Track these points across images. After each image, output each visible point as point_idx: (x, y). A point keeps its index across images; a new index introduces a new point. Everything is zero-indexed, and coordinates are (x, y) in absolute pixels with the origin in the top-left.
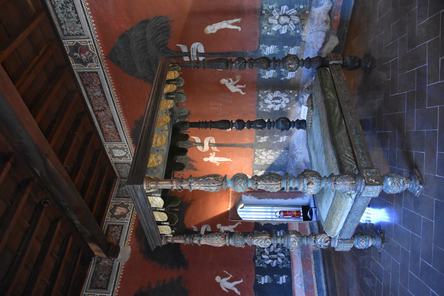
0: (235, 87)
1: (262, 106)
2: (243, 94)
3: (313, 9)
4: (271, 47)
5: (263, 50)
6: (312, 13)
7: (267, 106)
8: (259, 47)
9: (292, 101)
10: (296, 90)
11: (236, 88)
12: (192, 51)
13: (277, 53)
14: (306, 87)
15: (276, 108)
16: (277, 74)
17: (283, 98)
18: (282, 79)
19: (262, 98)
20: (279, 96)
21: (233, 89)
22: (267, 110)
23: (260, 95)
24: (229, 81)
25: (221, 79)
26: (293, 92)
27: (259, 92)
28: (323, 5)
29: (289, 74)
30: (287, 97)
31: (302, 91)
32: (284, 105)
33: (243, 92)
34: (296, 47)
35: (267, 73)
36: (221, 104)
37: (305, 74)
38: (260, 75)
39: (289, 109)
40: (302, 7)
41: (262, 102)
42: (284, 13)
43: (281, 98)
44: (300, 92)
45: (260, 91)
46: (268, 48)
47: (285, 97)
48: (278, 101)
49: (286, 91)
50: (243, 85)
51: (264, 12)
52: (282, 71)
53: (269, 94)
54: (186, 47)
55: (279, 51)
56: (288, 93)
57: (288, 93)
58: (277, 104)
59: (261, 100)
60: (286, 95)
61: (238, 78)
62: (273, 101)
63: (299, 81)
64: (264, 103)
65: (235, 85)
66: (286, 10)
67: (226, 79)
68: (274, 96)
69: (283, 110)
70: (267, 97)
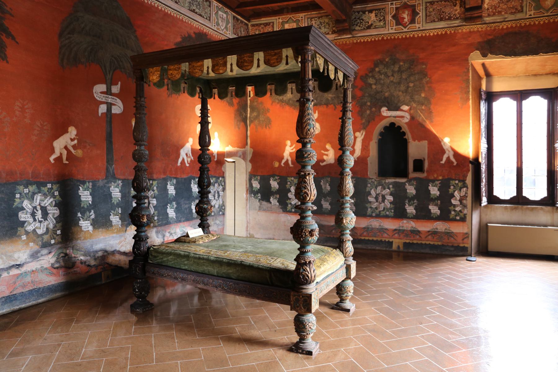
0: (63, 147)
1: (26, 191)
2: (52, 159)
3: (155, 230)
4: (119, 194)
5: (116, 184)
6: (152, 230)
7: (28, 199)
8: (119, 179)
9: (40, 239)
10: (62, 238)
11: (60, 149)
12: (113, 99)
13: (113, 202)
14: (68, 251)
15: (23, 216)
16: (86, 206)
17: (46, 223)
18: (79, 215)
19: (45, 189)
20: (50, 215)
21: (59, 145)
22: (17, 201)
23: (49, 186)
24: (72, 140)
25: (76, 128)
26: (58, 235)
27: (55, 184)
28: (158, 237)
29: (86, 222)
30: (47, 229)
31: (60, 248)
32: (30, 228)
33: (55, 159)
34: (120, 223)
35: (87, 193)
36: (28, 121)
37: (88, 244)
38: (84, 183)
39: (24, 237)
40: (156, 218)
41: (37, 191)
42: (151, 202)
43: (46, 219)
44: (59, 246)
45: (57, 185)
46: (117, 190)
47: (47, 225)
48: (41, 216)
49: (59, 225)
50: (67, 160)
51: (151, 182)
52: (90, 212)
53: (52, 200)
54: (117, 92)
55: (115, 203)
56: (56, 229)
57: (56, 229)
58: (33, 215)
59: (39, 188)
60: (51, 226)
61: (79, 153)
62: (38, 208)
63: (77, 239)
64: (34, 194)
65: (66, 148)
66: (153, 204)
67: (76, 135)
68: (48, 208)
69: (19, 229)
70: (45, 198)
